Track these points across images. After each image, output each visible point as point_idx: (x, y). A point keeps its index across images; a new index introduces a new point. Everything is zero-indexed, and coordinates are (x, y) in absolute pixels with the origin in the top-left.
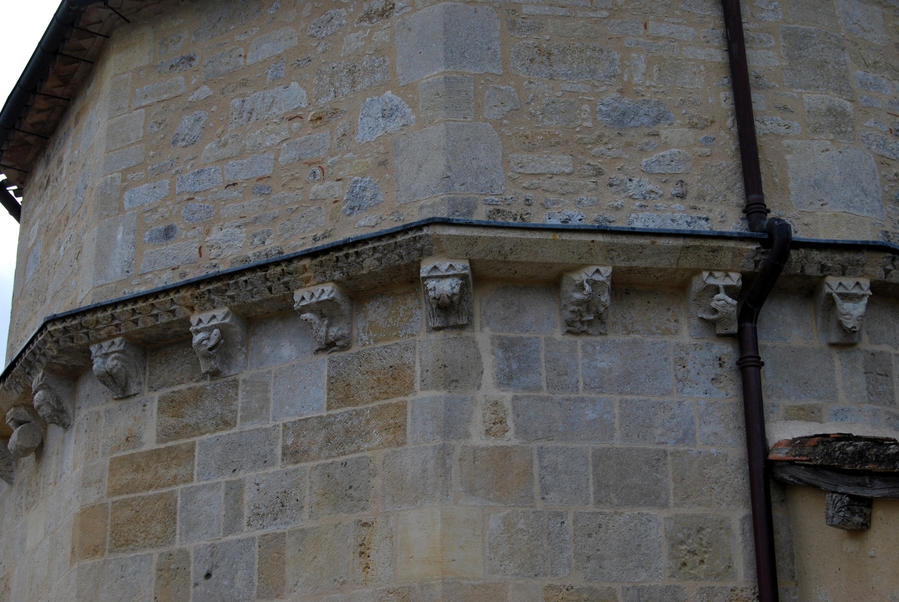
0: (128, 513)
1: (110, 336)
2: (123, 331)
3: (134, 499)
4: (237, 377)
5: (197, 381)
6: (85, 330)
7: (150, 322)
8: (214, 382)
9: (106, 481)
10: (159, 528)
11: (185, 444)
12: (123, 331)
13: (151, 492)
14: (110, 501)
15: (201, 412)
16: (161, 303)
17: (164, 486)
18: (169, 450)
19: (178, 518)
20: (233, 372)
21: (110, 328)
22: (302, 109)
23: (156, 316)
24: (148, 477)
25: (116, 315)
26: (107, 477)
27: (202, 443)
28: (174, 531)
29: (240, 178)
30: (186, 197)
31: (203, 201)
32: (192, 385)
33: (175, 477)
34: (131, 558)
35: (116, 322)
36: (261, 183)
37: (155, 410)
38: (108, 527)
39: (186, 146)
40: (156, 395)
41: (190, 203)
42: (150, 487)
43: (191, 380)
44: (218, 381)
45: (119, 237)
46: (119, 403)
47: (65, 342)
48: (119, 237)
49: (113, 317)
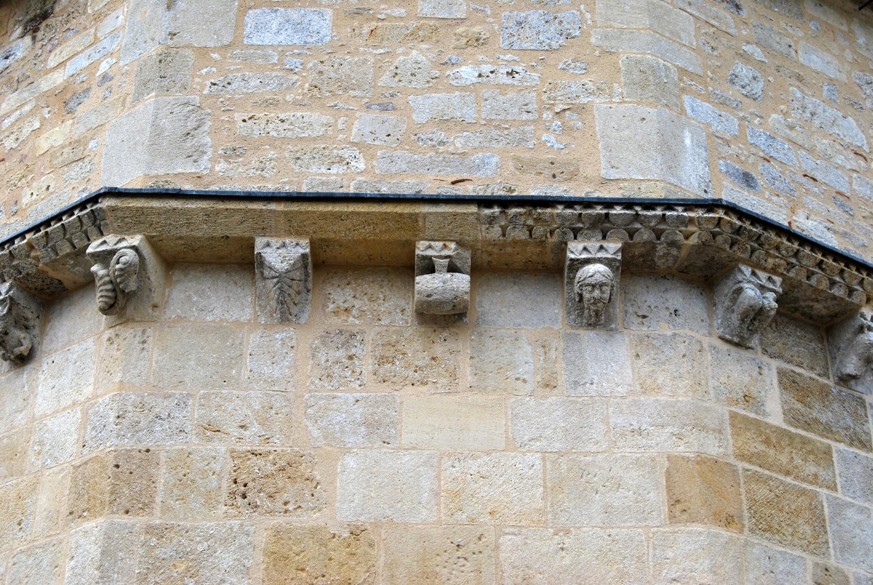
0: (763, 492)
1: (774, 271)
2: (791, 274)
3: (771, 478)
4: (864, 397)
5: (819, 375)
6: (756, 245)
7: (824, 285)
8: (838, 388)
9: (730, 437)
10: (807, 529)
11: (820, 442)
12: (791, 274)
13: (789, 480)
14: (741, 465)
15: (830, 413)
16: (851, 275)
17: (804, 480)
18: (805, 441)
19: (828, 528)
20: (859, 388)
21: (782, 262)
22: (864, 151)
23: (833, 283)
24: (784, 459)
25: (801, 254)
26: (730, 432)
27: (839, 451)
28: (827, 542)
29: (818, 175)
30: (761, 154)
31: (781, 172)
32: (813, 376)
33: (816, 476)
34: (781, 553)
35: (794, 261)
36: (839, 197)
37: (775, 381)
38: (743, 497)
39: (746, 96)
40: (775, 364)
41: (766, 164)
42: (788, 473)
43: (812, 369)
44: (844, 389)
45: (688, 142)
46: (725, 347)
47: (726, 241)
48: (688, 142)
49: (796, 254)
